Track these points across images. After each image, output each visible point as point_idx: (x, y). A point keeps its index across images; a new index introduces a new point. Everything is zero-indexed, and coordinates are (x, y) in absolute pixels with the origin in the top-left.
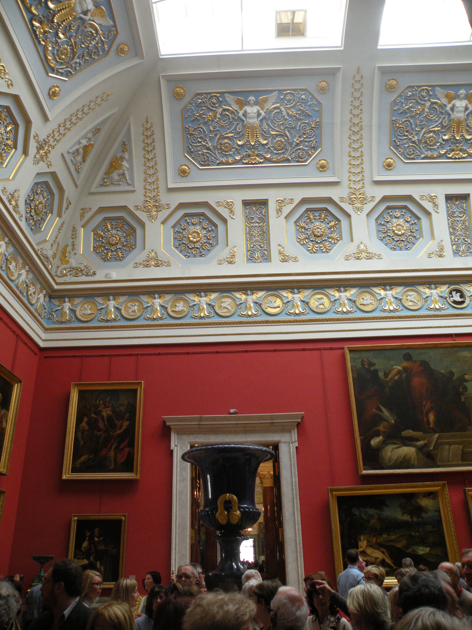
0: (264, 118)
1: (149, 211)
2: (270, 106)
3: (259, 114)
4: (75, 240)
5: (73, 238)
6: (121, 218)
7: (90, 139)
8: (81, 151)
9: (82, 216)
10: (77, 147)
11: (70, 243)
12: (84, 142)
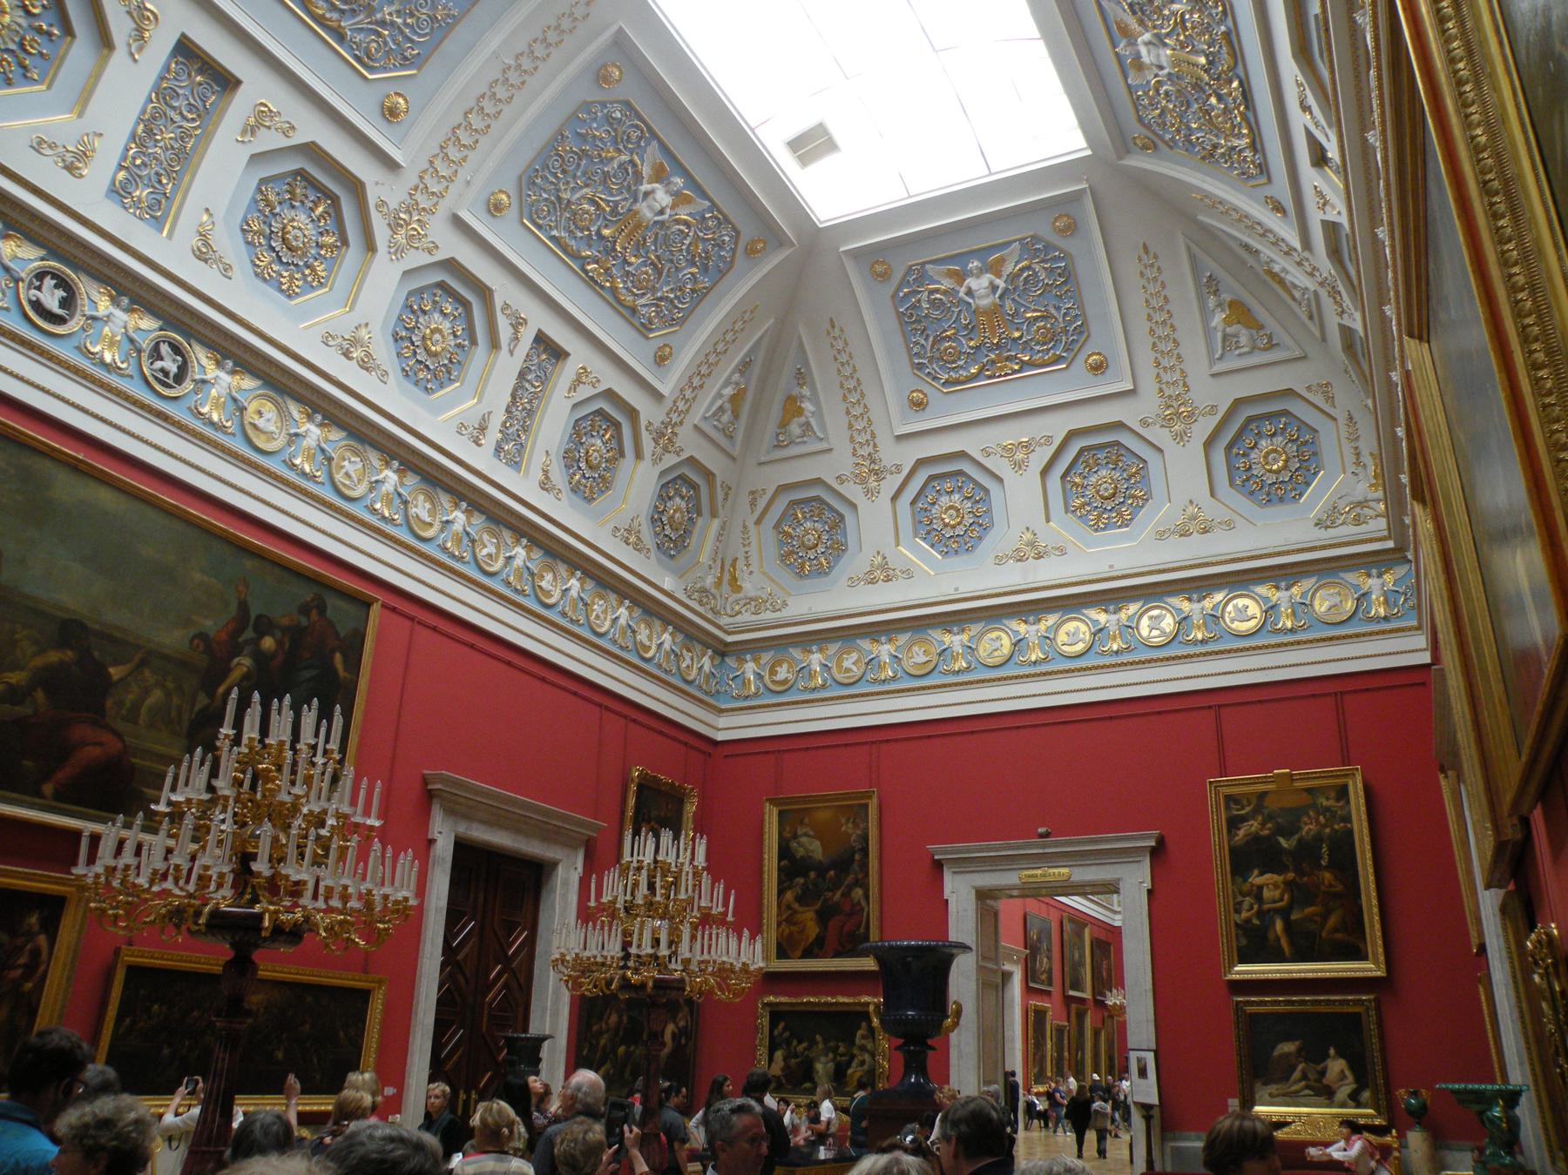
0: (1006, 291)
1: (864, 482)
2: (1009, 268)
3: (994, 288)
6: (818, 499)
7: (737, 384)
8: (728, 406)
9: (753, 504)
10: (719, 402)
11: (741, 557)
12: (728, 391)
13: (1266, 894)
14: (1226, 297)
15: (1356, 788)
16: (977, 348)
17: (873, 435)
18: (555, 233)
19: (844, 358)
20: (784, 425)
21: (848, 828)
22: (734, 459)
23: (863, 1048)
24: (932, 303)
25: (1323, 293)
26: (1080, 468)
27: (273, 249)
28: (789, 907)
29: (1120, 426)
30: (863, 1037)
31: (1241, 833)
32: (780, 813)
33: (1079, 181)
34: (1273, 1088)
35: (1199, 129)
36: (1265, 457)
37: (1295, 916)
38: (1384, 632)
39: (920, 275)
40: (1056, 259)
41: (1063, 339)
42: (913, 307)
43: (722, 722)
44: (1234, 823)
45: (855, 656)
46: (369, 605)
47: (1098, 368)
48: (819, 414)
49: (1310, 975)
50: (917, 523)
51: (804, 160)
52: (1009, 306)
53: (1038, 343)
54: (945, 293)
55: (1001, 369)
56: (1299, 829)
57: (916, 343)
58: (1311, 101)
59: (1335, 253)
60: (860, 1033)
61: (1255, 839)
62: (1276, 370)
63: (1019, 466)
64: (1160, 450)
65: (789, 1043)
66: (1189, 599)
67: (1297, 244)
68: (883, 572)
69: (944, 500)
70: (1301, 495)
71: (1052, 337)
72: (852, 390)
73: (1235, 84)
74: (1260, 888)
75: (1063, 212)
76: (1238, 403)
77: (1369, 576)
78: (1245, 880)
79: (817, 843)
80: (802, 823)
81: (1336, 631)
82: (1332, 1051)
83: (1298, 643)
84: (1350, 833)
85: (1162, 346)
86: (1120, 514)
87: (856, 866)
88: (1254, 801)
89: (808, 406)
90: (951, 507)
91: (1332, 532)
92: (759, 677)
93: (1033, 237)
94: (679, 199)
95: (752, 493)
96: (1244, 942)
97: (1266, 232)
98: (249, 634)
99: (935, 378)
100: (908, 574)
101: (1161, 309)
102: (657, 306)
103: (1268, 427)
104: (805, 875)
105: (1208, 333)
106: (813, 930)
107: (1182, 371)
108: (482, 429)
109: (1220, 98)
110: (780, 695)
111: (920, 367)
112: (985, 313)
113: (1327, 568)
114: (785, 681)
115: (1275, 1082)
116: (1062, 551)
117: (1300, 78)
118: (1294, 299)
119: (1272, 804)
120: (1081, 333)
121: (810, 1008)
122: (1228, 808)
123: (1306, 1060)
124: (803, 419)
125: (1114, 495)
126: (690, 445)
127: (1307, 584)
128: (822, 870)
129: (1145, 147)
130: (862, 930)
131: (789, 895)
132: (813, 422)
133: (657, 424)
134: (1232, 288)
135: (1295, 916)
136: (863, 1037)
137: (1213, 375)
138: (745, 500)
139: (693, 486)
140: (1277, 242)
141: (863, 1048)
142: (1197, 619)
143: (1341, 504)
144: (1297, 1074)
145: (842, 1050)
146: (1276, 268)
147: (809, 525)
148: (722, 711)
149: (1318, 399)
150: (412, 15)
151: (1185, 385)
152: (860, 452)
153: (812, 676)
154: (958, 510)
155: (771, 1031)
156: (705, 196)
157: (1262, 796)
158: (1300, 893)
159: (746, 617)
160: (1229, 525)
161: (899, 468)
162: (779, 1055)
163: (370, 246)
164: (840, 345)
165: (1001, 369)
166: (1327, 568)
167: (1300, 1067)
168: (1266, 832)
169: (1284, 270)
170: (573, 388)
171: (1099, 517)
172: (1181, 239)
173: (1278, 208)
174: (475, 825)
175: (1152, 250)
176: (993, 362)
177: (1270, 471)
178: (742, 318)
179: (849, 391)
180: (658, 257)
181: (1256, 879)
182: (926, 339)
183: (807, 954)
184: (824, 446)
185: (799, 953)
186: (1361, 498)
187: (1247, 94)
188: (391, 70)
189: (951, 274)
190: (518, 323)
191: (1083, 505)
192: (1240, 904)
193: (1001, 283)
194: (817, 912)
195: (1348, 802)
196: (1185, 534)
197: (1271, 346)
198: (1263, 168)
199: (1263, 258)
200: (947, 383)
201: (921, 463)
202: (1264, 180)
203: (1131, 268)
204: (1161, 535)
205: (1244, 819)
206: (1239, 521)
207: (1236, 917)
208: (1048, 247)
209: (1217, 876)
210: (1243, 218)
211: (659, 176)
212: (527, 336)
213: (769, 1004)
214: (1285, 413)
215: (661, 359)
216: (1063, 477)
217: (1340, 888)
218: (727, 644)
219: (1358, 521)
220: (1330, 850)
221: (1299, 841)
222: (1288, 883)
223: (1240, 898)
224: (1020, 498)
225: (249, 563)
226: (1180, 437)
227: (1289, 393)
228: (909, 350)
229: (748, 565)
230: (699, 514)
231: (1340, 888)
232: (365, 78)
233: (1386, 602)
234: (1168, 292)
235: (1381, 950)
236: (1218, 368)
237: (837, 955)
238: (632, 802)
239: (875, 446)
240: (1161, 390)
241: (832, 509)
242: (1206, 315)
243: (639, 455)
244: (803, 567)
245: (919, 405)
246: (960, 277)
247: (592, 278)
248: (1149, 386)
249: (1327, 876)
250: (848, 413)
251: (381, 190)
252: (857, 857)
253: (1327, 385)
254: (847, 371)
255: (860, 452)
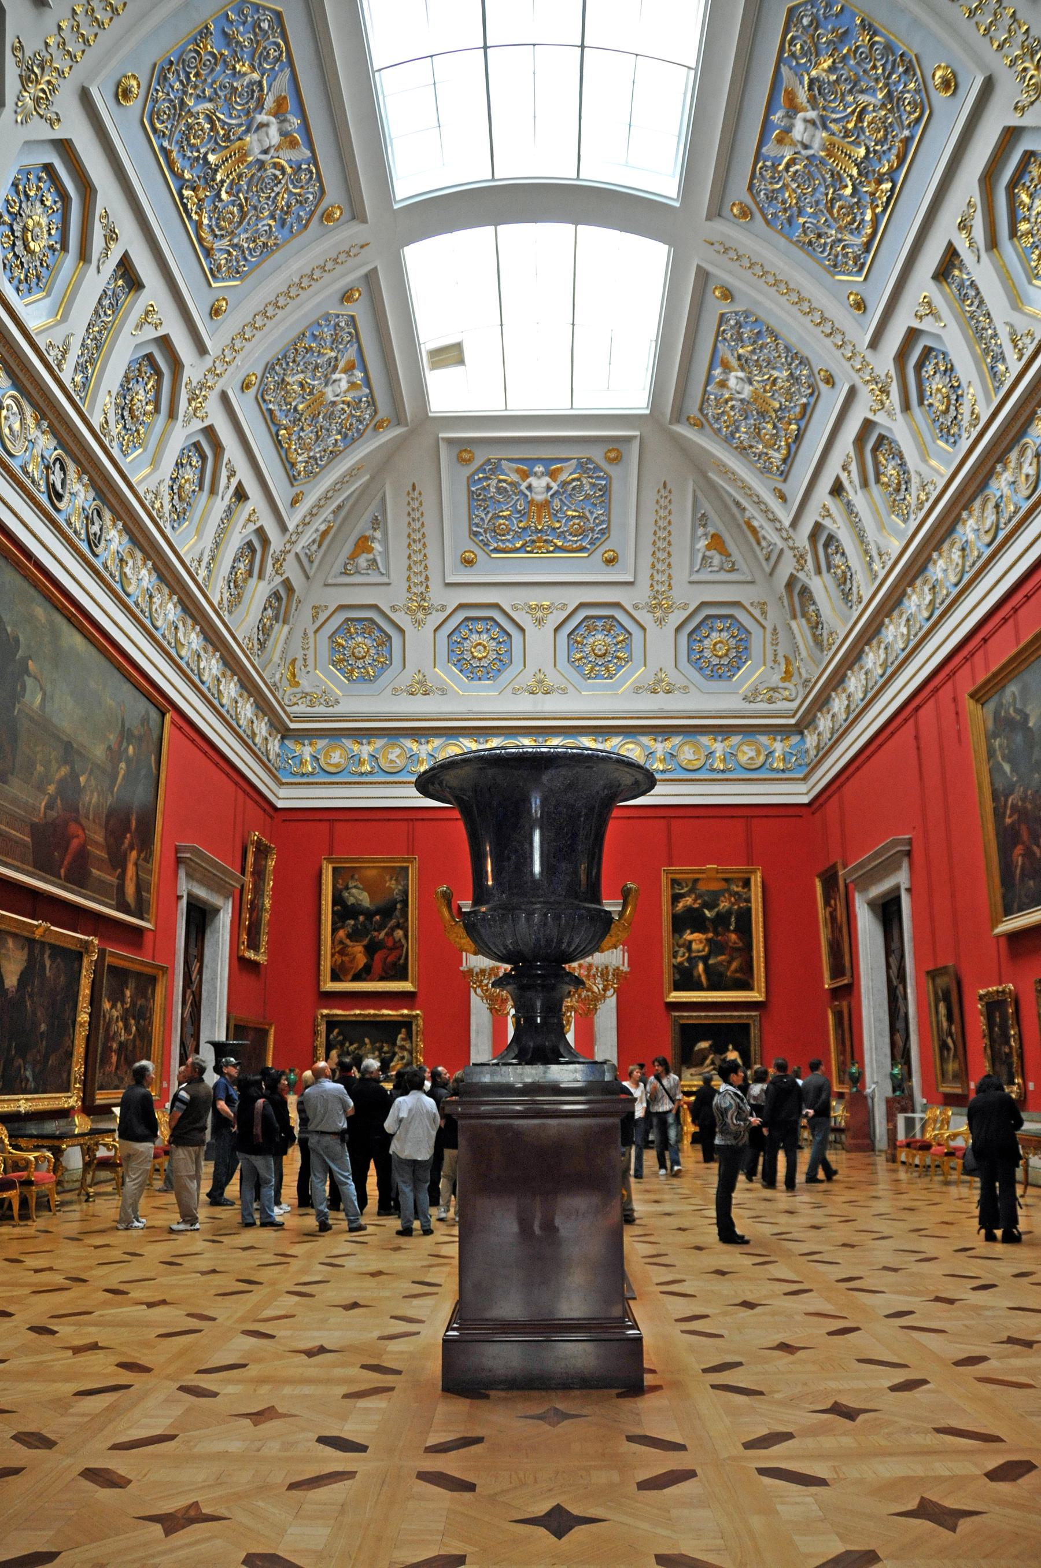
0: (557, 492)
2: (564, 477)
4: (306, 652)
5: (304, 649)
6: (371, 620)
8: (318, 539)
9: (315, 618)
10: (315, 536)
11: (300, 657)
12: (323, 527)
13: (694, 946)
14: (711, 530)
15: (756, 880)
16: (524, 529)
17: (427, 578)
18: (271, 406)
19: (417, 515)
20: (353, 557)
21: (392, 884)
22: (308, 578)
23: (403, 1048)
24: (499, 490)
25: (788, 554)
26: (582, 631)
27: (123, 417)
28: (341, 942)
29: (617, 605)
30: (403, 1039)
31: (681, 905)
32: (334, 869)
33: (634, 429)
34: (693, 1070)
35: (746, 433)
36: (715, 645)
37: (711, 962)
38: (781, 779)
39: (496, 467)
40: (599, 478)
41: (590, 536)
42: (484, 488)
43: (282, 792)
44: (676, 898)
45: (398, 751)
46: (163, 715)
47: (610, 561)
48: (386, 553)
49: (720, 1000)
50: (451, 651)
51: (434, 366)
52: (556, 504)
53: (570, 534)
54: (511, 484)
55: (540, 548)
56: (718, 905)
57: (477, 516)
58: (854, 467)
59: (813, 537)
60: (400, 1036)
61: (689, 910)
62: (733, 588)
63: (540, 621)
64: (644, 629)
65: (342, 1044)
66: (655, 740)
67: (787, 523)
68: (422, 688)
69: (475, 637)
70: (734, 675)
71: (582, 532)
72: (416, 540)
73: (794, 427)
74: (690, 942)
75: (615, 450)
76: (704, 604)
77: (775, 740)
78: (681, 937)
79: (365, 894)
80: (352, 877)
81: (752, 773)
82: (731, 1047)
83: (727, 780)
84: (749, 909)
85: (659, 555)
86: (607, 669)
87: (397, 913)
88: (690, 885)
89: (377, 546)
90: (480, 644)
91: (753, 706)
92: (316, 759)
93: (588, 459)
94: (353, 385)
95: (315, 607)
96: (677, 977)
97: (759, 502)
98: (125, 744)
99: (487, 545)
100: (443, 691)
101: (665, 528)
102: (307, 462)
103: (719, 625)
104: (356, 918)
105: (693, 551)
106: (361, 960)
107: (670, 575)
108: (200, 561)
109: (775, 427)
110: (332, 777)
111: (476, 534)
112: (537, 505)
113: (749, 731)
114: (336, 765)
115: (695, 1066)
116: (564, 691)
117: (852, 454)
118: (759, 543)
119: (702, 887)
120: (604, 534)
121: (360, 1019)
122: (673, 888)
123: (715, 1053)
124: (371, 556)
125: (604, 655)
126: (292, 571)
127: (735, 740)
128: (369, 914)
129: (695, 425)
130: (402, 961)
131: (341, 933)
132: (379, 559)
133: (278, 552)
134: (716, 524)
135: (711, 962)
136: (403, 1039)
137: (690, 582)
138: (307, 613)
139: (279, 598)
140: (774, 520)
141: (403, 1048)
142: (659, 754)
143: (760, 687)
144: (708, 1061)
145: (386, 1049)
146: (755, 524)
147: (360, 639)
148: (283, 784)
149: (757, 613)
150: (254, 241)
151: (669, 585)
152: (414, 590)
153: (361, 763)
154: (485, 647)
155: (328, 1036)
156: (369, 386)
157: (696, 881)
158: (715, 947)
159: (302, 708)
160: (685, 690)
161: (443, 608)
162: (334, 1053)
163: (172, 415)
164: (416, 505)
165: (540, 548)
166: (749, 731)
167: (711, 1056)
168: (696, 906)
169: (761, 527)
170: (244, 527)
171: (592, 670)
172: (691, 484)
173: (783, 497)
174: (195, 884)
175: (668, 487)
176: (534, 541)
177: (716, 656)
178: (352, 474)
179: (414, 541)
180: (321, 427)
181: (688, 936)
182: (486, 515)
183: (356, 978)
184: (385, 580)
185: (350, 977)
186: (774, 685)
187: (799, 437)
188: (227, 281)
189: (517, 471)
190: (232, 473)
191: (580, 659)
192: (677, 952)
193: (555, 486)
194: (364, 946)
195: (750, 890)
196: (654, 692)
197: (732, 570)
198: (785, 475)
199: (747, 514)
200: (496, 550)
201: (461, 606)
202: (781, 479)
203: (650, 496)
204: (637, 690)
205: (683, 896)
206: (692, 689)
207: (674, 961)
208: (598, 468)
209: (665, 934)
210: (745, 488)
211: (349, 369)
212: (234, 482)
213: (327, 1016)
214: (730, 616)
215: (294, 502)
216: (569, 635)
217: (741, 945)
218: (288, 729)
219: (770, 701)
220: (737, 919)
221: (718, 914)
222: (709, 941)
223: (677, 949)
224: (540, 645)
225: (127, 687)
226: (660, 621)
227: (737, 604)
228: (470, 519)
229: (305, 666)
230: (277, 620)
231: (741, 945)
232: (210, 285)
233: (784, 759)
234: (672, 518)
235: (763, 985)
236: (696, 577)
237: (382, 979)
238: (250, 859)
239: (427, 587)
240: (652, 586)
241: (381, 630)
242: (694, 538)
243: (261, 577)
244: (352, 672)
245: (468, 563)
246: (525, 475)
247: (280, 442)
248: (644, 581)
249: (733, 937)
250: (409, 557)
251: (193, 370)
252: (399, 906)
253: (764, 604)
254: (418, 525)
255: (414, 590)
